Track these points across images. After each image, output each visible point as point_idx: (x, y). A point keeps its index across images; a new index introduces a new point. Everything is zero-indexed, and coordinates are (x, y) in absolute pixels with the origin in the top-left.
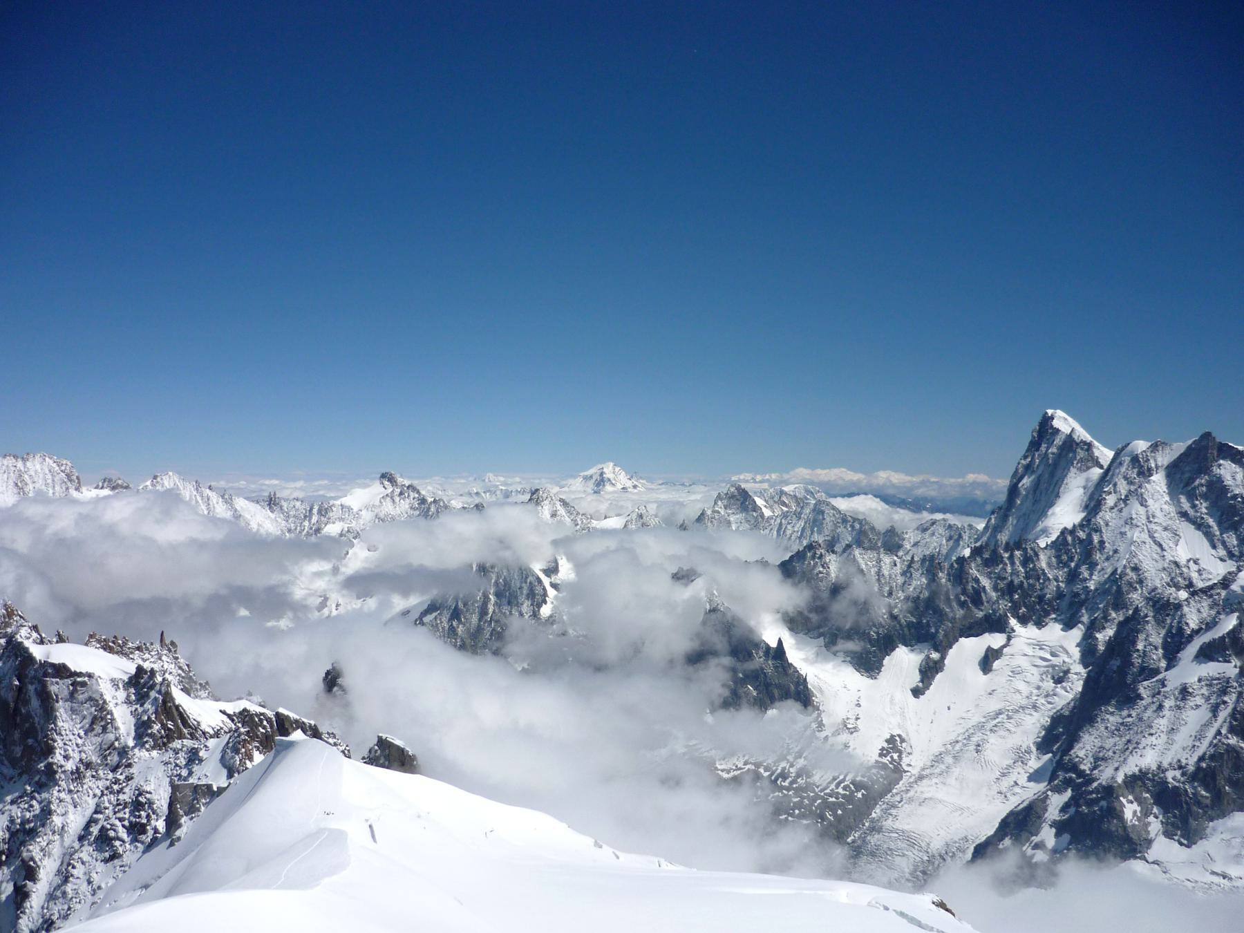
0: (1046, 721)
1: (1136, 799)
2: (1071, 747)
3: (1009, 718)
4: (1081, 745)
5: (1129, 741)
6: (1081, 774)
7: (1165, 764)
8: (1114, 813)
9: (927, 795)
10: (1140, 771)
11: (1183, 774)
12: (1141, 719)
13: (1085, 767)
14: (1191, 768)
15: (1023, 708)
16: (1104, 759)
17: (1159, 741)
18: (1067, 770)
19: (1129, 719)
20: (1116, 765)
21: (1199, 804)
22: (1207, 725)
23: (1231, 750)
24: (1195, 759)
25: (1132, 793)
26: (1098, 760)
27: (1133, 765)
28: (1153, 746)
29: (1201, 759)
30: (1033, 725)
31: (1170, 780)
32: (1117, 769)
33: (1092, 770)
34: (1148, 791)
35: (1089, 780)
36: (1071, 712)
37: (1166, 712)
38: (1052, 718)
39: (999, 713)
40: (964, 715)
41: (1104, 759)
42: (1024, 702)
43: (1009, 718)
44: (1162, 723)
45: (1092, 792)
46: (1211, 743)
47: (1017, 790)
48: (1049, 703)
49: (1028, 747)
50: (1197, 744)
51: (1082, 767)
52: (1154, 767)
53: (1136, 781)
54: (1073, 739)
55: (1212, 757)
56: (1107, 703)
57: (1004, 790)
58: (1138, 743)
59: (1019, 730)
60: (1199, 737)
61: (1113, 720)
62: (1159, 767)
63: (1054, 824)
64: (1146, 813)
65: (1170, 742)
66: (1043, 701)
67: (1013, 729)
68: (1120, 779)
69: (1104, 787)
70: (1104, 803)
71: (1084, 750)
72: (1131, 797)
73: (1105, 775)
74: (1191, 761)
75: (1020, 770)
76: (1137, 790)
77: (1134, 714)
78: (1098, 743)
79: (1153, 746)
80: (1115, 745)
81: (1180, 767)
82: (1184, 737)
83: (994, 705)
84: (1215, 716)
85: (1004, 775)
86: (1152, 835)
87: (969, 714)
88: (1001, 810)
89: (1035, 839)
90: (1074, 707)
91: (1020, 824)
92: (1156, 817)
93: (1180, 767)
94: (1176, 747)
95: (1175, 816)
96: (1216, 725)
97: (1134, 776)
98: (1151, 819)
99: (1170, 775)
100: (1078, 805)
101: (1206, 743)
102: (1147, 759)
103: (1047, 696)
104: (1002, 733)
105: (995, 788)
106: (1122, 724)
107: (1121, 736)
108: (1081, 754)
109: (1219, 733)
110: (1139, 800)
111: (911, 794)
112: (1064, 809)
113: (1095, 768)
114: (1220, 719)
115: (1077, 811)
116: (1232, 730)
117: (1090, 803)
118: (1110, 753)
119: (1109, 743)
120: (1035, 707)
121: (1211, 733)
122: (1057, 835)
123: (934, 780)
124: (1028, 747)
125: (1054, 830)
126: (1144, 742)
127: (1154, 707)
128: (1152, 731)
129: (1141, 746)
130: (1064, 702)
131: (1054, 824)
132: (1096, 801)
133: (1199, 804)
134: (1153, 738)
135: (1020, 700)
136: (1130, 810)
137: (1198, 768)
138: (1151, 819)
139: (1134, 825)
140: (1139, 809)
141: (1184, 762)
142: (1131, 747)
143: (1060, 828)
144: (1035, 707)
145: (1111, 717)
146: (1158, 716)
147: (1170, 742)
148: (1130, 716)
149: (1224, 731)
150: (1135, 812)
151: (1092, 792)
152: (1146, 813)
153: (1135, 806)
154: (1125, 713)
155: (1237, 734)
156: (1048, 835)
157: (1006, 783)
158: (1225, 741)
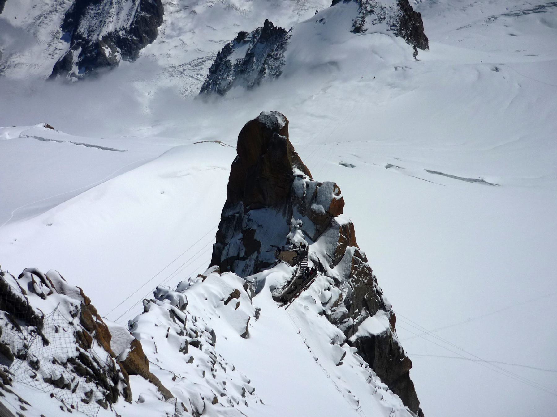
0: (63, 16)
1: (109, 46)
2: (77, 28)
3: (45, 18)
4: (81, 26)
5: (101, 21)
6: (84, 39)
7: (118, 29)
8: (101, 54)
9: (16, 62)
10: (108, 33)
11: (126, 32)
12: (104, 10)
13: (85, 36)
14: (128, 29)
15: (51, 12)
16: (92, 31)
17: (113, 19)
18: (77, 39)
19: (99, 11)
20: (98, 33)
21: (134, 43)
22: (131, 9)
23: (143, 18)
24: (129, 24)
25: (107, 44)
26: (90, 32)
27: (104, 32)
28: (112, 22)
29: (132, 24)
30: (57, 19)
31: (121, 35)
32: (98, 35)
33: (88, 37)
34: (113, 42)
35: (88, 41)
36: (73, 10)
37: (114, 5)
38: (65, 15)
39: (40, 16)
40: (24, 20)
41: (92, 31)
42: (51, 9)
43: (45, 18)
44: (113, 11)
45: (90, 47)
46: (135, 16)
47: (57, 51)
48: (62, 7)
49: (58, 30)
50: (129, 18)
51: (84, 36)
52: (114, 31)
53: (108, 38)
54: (77, 24)
55: (136, 22)
56: (89, 5)
57: (51, 53)
58: (105, 22)
59: (52, 23)
60: (129, 15)
61: (92, 12)
62: (116, 31)
63: (77, 64)
64: (114, 51)
65: (118, 19)
66: (59, 7)
67: (48, 23)
68: (101, 39)
69: (95, 44)
70: (96, 51)
71: (83, 27)
72: (106, 46)
73: (94, 38)
74: (128, 25)
75: (56, 42)
76: (109, 42)
77: (101, 8)
78: (88, 24)
79: (112, 22)
80: (96, 24)
81: (124, 29)
82: (123, 15)
83: (37, 13)
84: (134, 4)
85: (49, 45)
86: (118, 60)
87: (26, 19)
88: (52, 62)
89: (71, 72)
90: (74, 8)
91: (62, 66)
92: (118, 52)
93: (124, 29)
94: (121, 21)
95: (125, 51)
96: (135, 8)
97: (106, 36)
98: (117, 54)
99: (121, 33)
100: (85, 54)
101: (132, 16)
102: (110, 27)
103: (60, 4)
104: (44, 26)
105: (47, 53)
106: (97, 13)
107: (97, 19)
108: (82, 30)
109: (137, 11)
110: (110, 47)
111: (9, 63)
112: (79, 57)
113: (89, 36)
114: (137, 5)
115: (86, 57)
116: (142, 9)
117: (90, 52)
118: (94, 28)
119: (93, 22)
120: (56, 11)
121: (134, 13)
122: (79, 69)
123: (18, 54)
124: (58, 30)
125: (77, 67)
126: (107, 20)
127: (109, 4)
128: (110, 15)
129: (107, 23)
130: (69, 6)
131: (77, 64)
132: (93, 50)
133: (134, 43)
134: (111, 18)
135: (47, 8)
136: (107, 52)
137: (131, 29)
138: (117, 54)
139: (110, 58)
140: (111, 50)
141: (125, 26)
142: (102, 23)
143: (80, 65)
144: (56, 11)
145: (92, 11)
146: (111, 8)
147: (118, 19)
148: (99, 9)
149: (139, 11)
150: (109, 52)
151: (90, 47)
152: (114, 51)
153: (109, 50)
154: (97, 8)
155: (144, 11)
156: (75, 69)
157: (51, 49)
158: (140, 15)
